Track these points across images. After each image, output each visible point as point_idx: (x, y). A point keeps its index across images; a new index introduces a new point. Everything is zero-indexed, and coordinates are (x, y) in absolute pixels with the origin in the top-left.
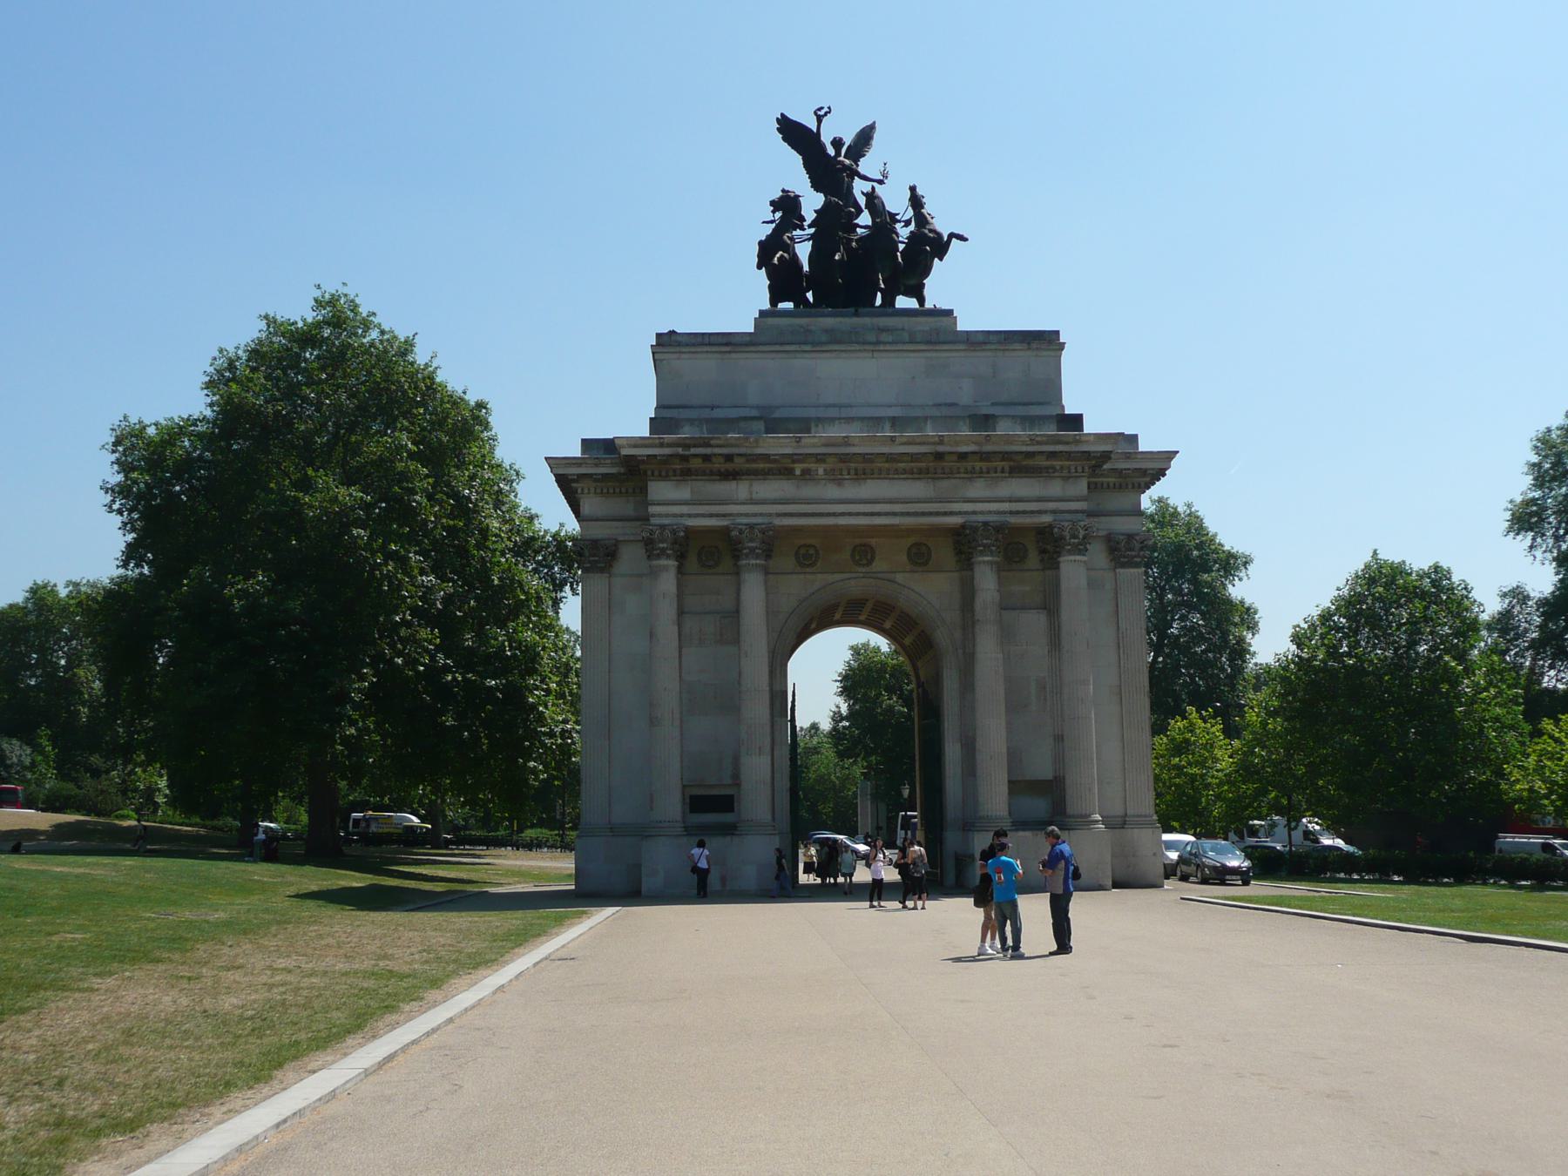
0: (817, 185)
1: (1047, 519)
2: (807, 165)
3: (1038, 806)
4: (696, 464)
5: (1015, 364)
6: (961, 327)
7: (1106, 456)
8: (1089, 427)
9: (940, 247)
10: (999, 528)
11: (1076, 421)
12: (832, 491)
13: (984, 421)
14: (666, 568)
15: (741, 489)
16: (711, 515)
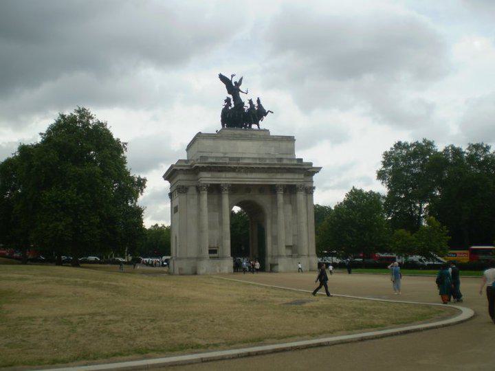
0: (229, 93)
1: (294, 183)
2: (227, 87)
3: (289, 252)
4: (212, 168)
5: (284, 145)
6: (271, 134)
7: (308, 169)
8: (304, 161)
9: (265, 114)
10: (283, 185)
11: (301, 160)
12: (245, 176)
13: (281, 159)
14: (203, 194)
15: (223, 175)
16: (216, 181)
